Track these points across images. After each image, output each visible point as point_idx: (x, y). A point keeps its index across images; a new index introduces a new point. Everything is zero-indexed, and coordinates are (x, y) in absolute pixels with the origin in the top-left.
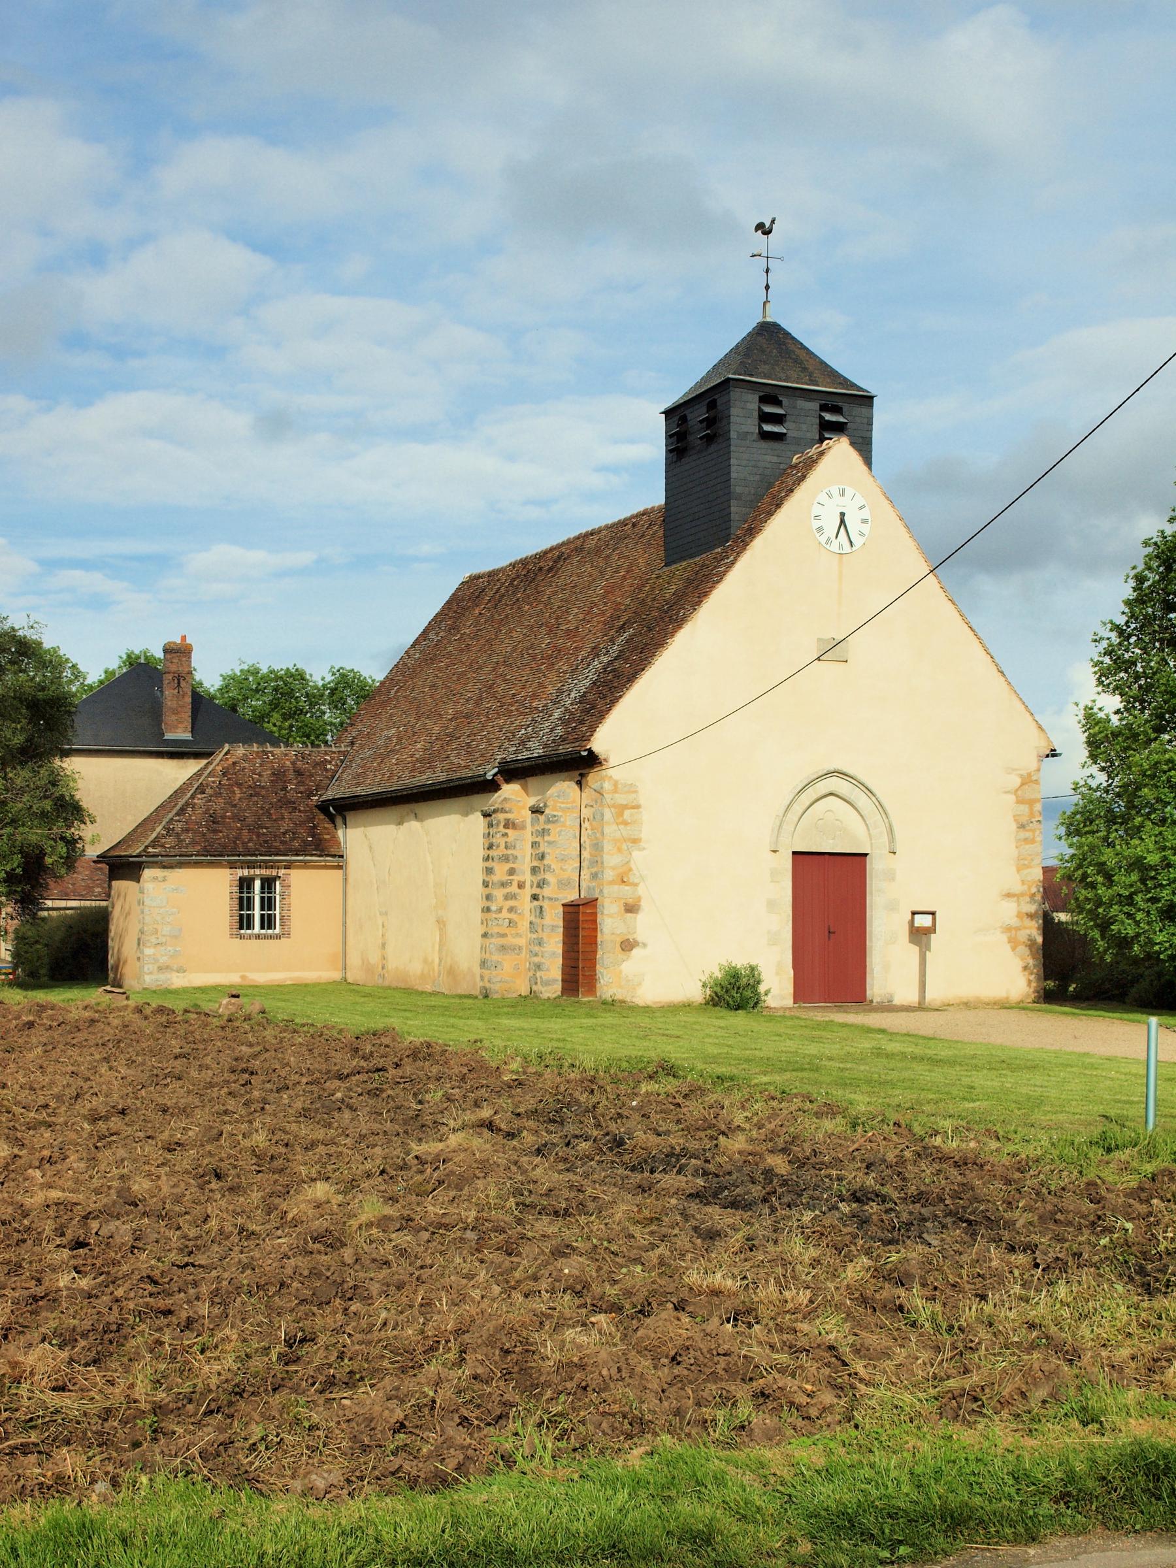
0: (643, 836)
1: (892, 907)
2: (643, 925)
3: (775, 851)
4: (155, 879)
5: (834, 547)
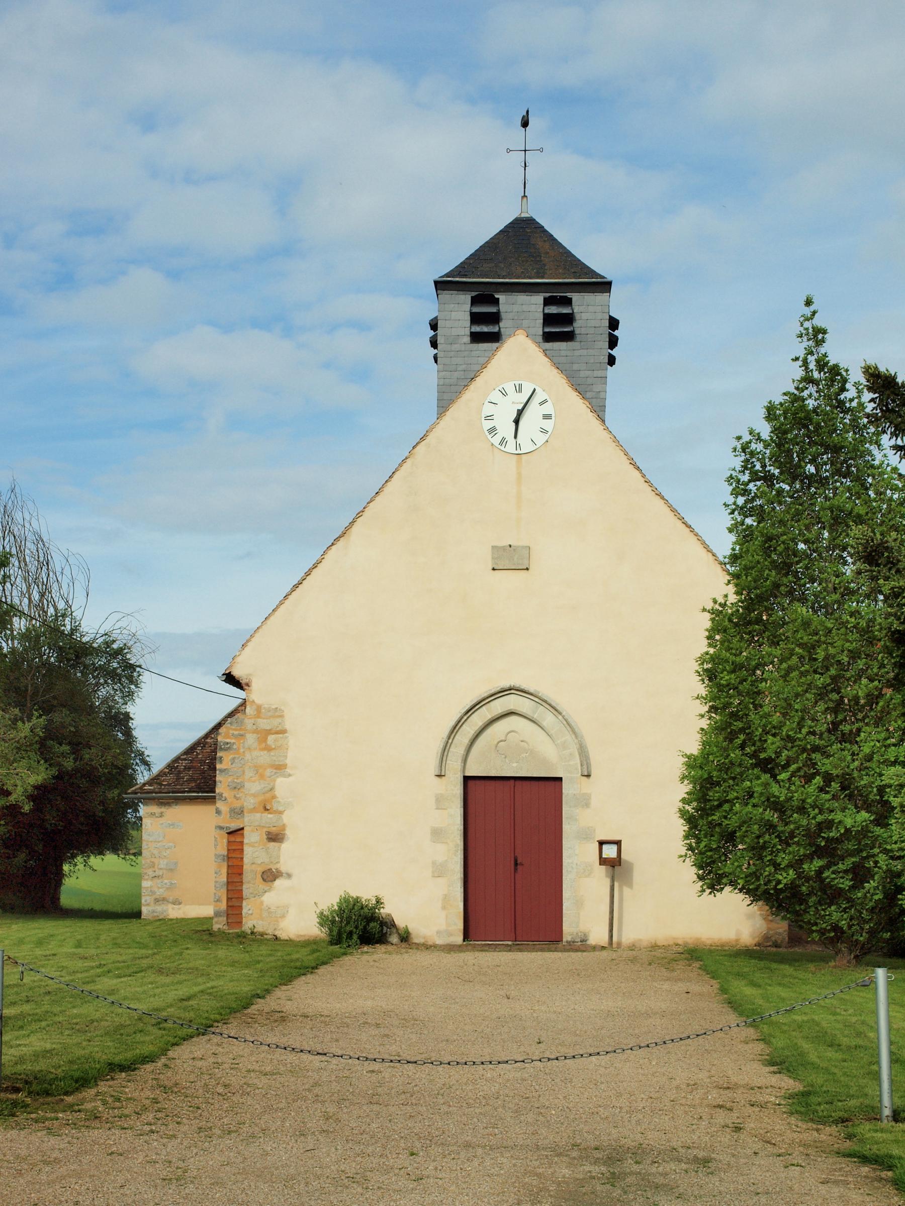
0: (288, 761)
1: (585, 835)
2: (287, 855)
3: (439, 776)
4: (153, 814)
5: (511, 447)
